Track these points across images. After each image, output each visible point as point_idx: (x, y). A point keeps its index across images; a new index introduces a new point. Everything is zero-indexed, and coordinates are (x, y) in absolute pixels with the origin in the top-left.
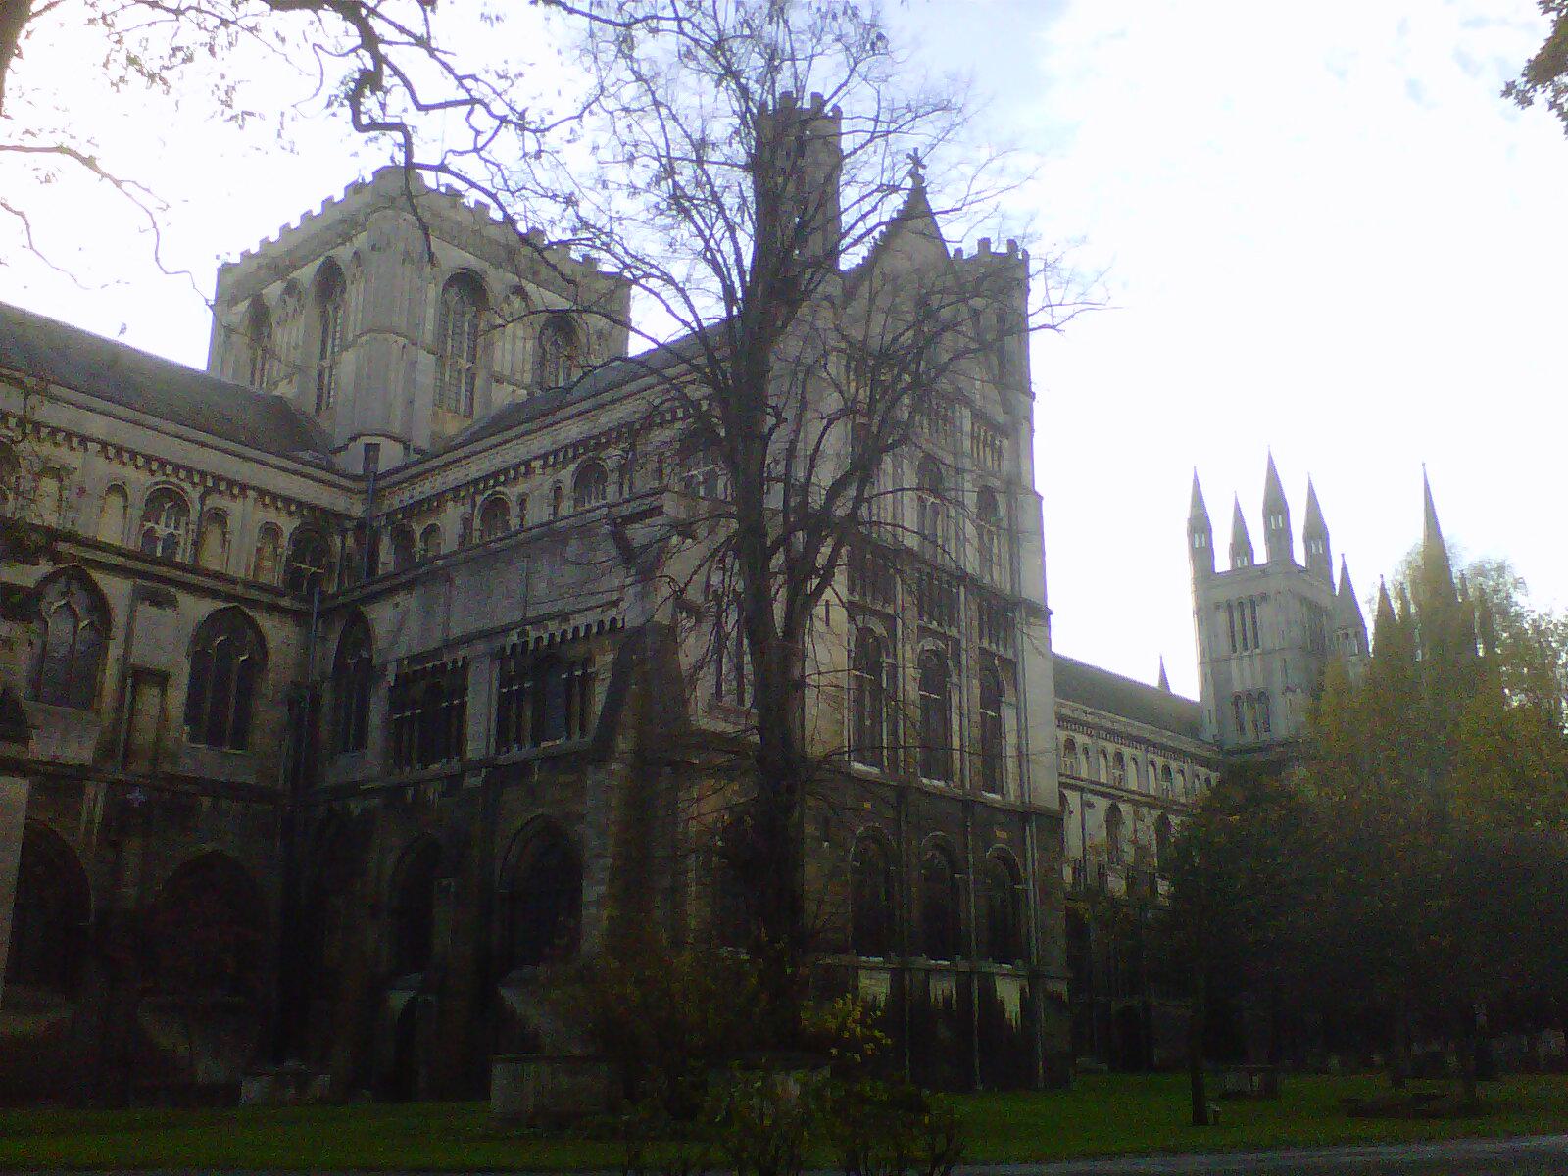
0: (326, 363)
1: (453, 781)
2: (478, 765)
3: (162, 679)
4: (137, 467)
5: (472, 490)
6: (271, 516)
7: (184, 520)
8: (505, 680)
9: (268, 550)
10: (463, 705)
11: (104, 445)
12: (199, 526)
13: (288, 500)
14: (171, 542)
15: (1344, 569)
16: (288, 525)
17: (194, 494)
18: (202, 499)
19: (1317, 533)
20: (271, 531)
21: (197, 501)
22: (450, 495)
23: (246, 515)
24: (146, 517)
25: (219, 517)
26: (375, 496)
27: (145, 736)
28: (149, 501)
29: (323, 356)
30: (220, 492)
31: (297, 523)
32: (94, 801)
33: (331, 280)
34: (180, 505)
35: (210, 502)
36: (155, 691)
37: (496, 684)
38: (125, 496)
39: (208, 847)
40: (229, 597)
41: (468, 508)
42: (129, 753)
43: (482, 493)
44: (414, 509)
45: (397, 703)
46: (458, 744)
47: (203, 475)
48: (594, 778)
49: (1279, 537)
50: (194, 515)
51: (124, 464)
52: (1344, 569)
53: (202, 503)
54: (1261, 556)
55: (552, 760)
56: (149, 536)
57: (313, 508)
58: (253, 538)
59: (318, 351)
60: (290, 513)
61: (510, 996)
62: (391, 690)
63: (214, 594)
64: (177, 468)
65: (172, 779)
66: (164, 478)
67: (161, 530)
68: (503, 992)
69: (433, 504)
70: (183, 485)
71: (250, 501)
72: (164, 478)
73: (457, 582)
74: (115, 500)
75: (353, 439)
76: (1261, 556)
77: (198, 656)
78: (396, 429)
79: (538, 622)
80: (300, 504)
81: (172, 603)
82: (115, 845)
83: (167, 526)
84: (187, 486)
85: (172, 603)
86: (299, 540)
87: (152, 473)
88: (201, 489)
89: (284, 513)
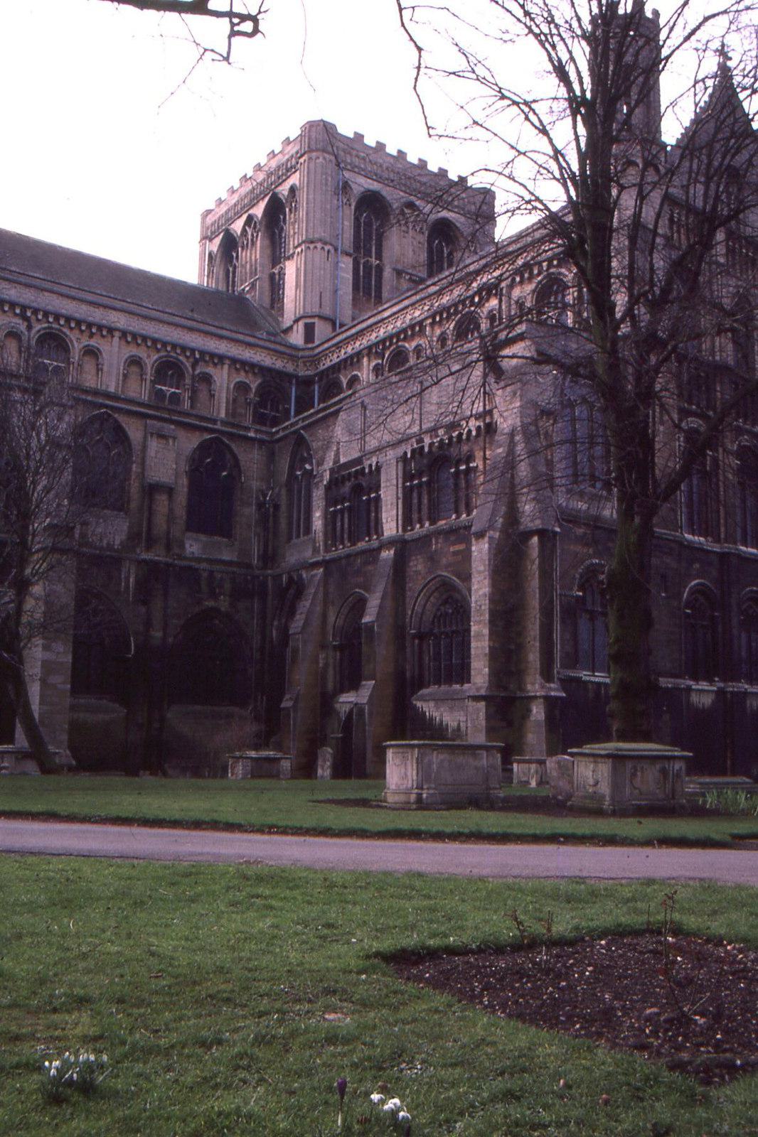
3: (170, 491)
4: (148, 347)
6: (242, 377)
8: (408, 476)
10: (378, 499)
20: (242, 387)
21: (190, 369)
22: (365, 352)
23: (223, 379)
25: (207, 379)
26: (315, 360)
30: (205, 361)
31: (259, 381)
32: (130, 576)
33: (276, 210)
34: (181, 375)
37: (400, 481)
43: (389, 348)
44: (337, 368)
45: (331, 500)
46: (378, 526)
47: (193, 351)
50: (188, 381)
51: (138, 345)
53: (194, 369)
62: (328, 488)
64: (174, 346)
68: (419, 704)
69: (353, 361)
78: (327, 311)
79: (433, 431)
86: (262, 391)
88: (191, 360)
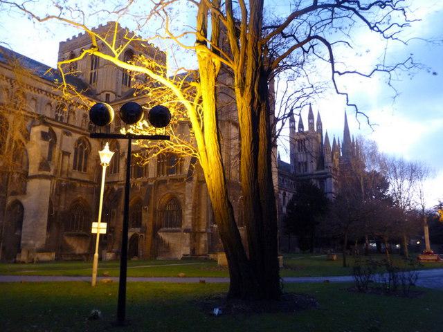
0: (93, 71)
1: (144, 184)
2: (153, 179)
3: (68, 154)
11: (46, 92)
14: (62, 118)
15: (327, 133)
19: (319, 123)
24: (56, 111)
27: (65, 168)
29: (92, 69)
36: (67, 157)
39: (79, 196)
40: (83, 134)
42: (62, 172)
46: (146, 174)
48: (189, 185)
49: (311, 125)
52: (327, 133)
54: (306, 128)
55: (174, 180)
56: (57, 116)
59: (90, 67)
61: (161, 234)
63: (79, 133)
65: (71, 179)
67: (59, 115)
74: (49, 107)
75: (103, 92)
76: (306, 128)
77: (76, 149)
81: (71, 135)
82: (59, 195)
85: (71, 135)
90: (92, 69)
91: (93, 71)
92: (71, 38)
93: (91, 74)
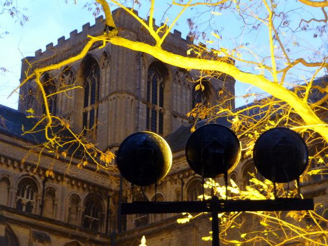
0: (89, 108)
4: (14, 168)
5: (181, 176)
7: (35, 194)
9: (74, 209)
12: (43, 197)
13: (83, 182)
14: (29, 206)
16: (83, 195)
17: (40, 181)
18: (44, 182)
20: (75, 199)
21: (41, 185)
24: (18, 194)
25: (51, 192)
28: (19, 185)
29: (86, 105)
31: (87, 193)
34: (35, 187)
35: (49, 184)
38: (9, 183)
40: (73, 237)
41: (178, 186)
43: (188, 177)
56: (19, 203)
57: (94, 186)
58: (67, 203)
59: (82, 102)
60: (84, 188)
66: (26, 173)
67: (25, 200)
70: (35, 176)
71: (65, 184)
72: (26, 173)
73: (200, 229)
80: (89, 184)
83: (27, 198)
84: (37, 176)
86: (89, 202)
87: (21, 170)
88: (43, 178)
89: (81, 189)
90: (86, 105)
91: (89, 108)
92: (44, 49)
93: (85, 114)
